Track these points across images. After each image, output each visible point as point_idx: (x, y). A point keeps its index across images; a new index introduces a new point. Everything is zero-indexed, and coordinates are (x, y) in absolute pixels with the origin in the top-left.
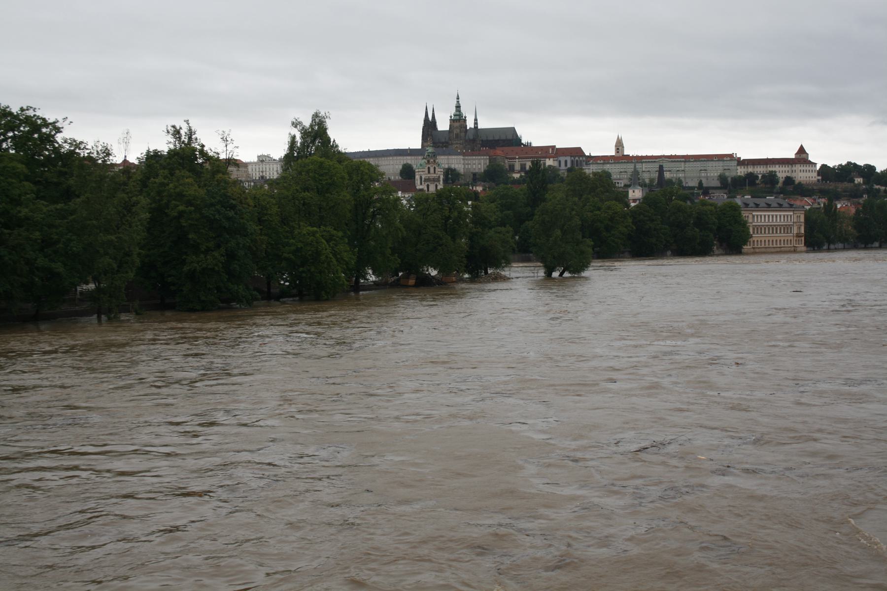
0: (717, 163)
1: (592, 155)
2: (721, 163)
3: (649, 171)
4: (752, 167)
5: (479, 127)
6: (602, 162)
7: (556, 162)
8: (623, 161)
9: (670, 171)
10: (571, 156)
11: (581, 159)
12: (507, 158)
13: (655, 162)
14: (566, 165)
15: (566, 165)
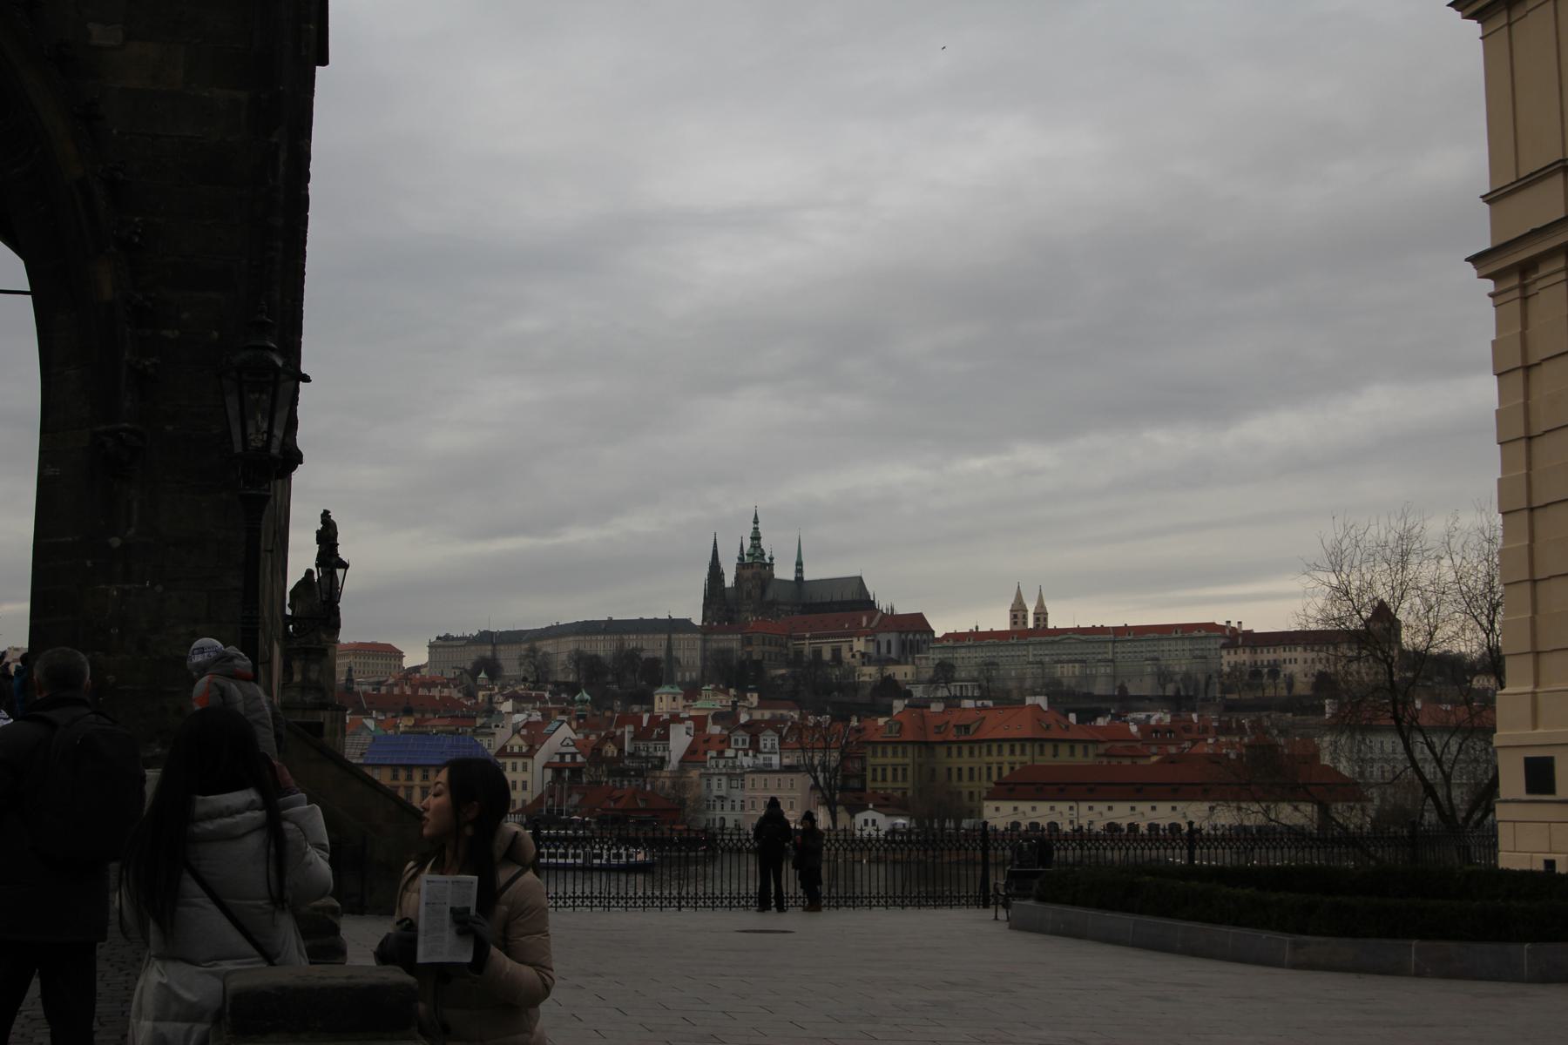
0: (1180, 642)
1: (980, 630)
2: (1187, 642)
3: (1037, 663)
4: (1248, 650)
5: (807, 576)
6: (951, 643)
7: (871, 643)
8: (991, 641)
9: (1084, 661)
10: (901, 632)
11: (918, 637)
12: (790, 637)
13: (1053, 642)
14: (889, 651)
15: (889, 651)
